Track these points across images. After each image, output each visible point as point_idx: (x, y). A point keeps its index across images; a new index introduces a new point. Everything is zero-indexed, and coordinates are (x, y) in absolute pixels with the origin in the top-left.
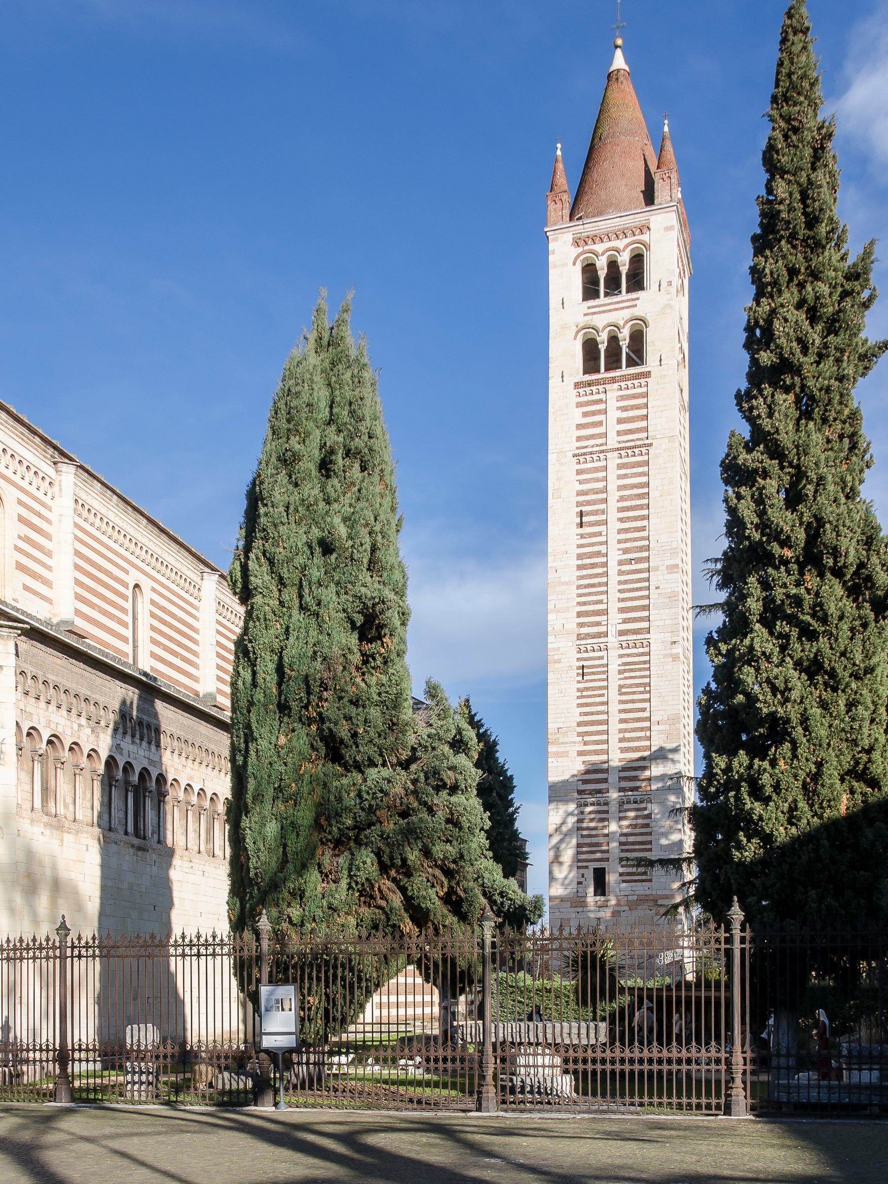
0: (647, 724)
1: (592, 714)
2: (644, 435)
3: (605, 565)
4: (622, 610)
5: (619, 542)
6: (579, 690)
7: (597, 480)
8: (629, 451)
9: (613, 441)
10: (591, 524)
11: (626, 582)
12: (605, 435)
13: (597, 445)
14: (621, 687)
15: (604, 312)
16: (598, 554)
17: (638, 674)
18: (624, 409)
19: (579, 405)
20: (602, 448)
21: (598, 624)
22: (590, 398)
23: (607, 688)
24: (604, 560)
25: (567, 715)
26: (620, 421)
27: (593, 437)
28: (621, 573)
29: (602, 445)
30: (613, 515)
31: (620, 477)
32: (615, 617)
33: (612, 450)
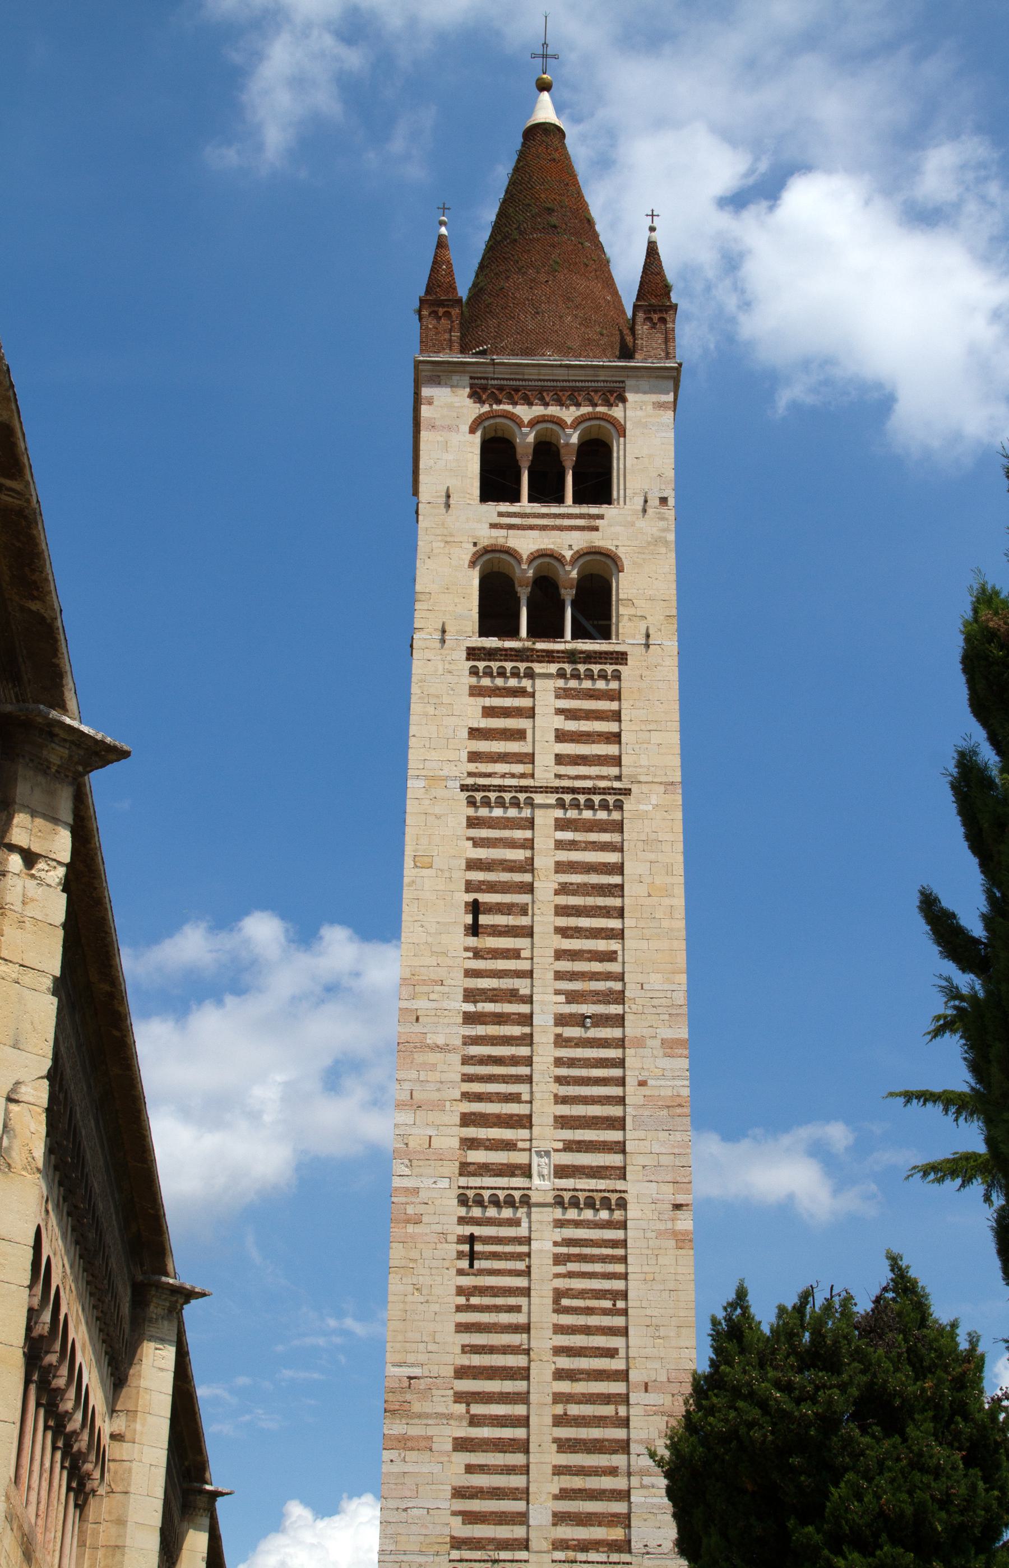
2: (614, 771)
3: (527, 1019)
4: (563, 1122)
5: (559, 976)
7: (512, 844)
8: (582, 798)
9: (545, 771)
10: (497, 931)
11: (572, 1063)
12: (529, 758)
13: (513, 776)
14: (559, 1294)
16: (513, 996)
17: (598, 1267)
18: (571, 714)
20: (524, 782)
21: (509, 1146)
23: (526, 1292)
24: (524, 1009)
25: (432, 1347)
26: (561, 736)
28: (561, 1041)
29: (523, 776)
31: (560, 845)
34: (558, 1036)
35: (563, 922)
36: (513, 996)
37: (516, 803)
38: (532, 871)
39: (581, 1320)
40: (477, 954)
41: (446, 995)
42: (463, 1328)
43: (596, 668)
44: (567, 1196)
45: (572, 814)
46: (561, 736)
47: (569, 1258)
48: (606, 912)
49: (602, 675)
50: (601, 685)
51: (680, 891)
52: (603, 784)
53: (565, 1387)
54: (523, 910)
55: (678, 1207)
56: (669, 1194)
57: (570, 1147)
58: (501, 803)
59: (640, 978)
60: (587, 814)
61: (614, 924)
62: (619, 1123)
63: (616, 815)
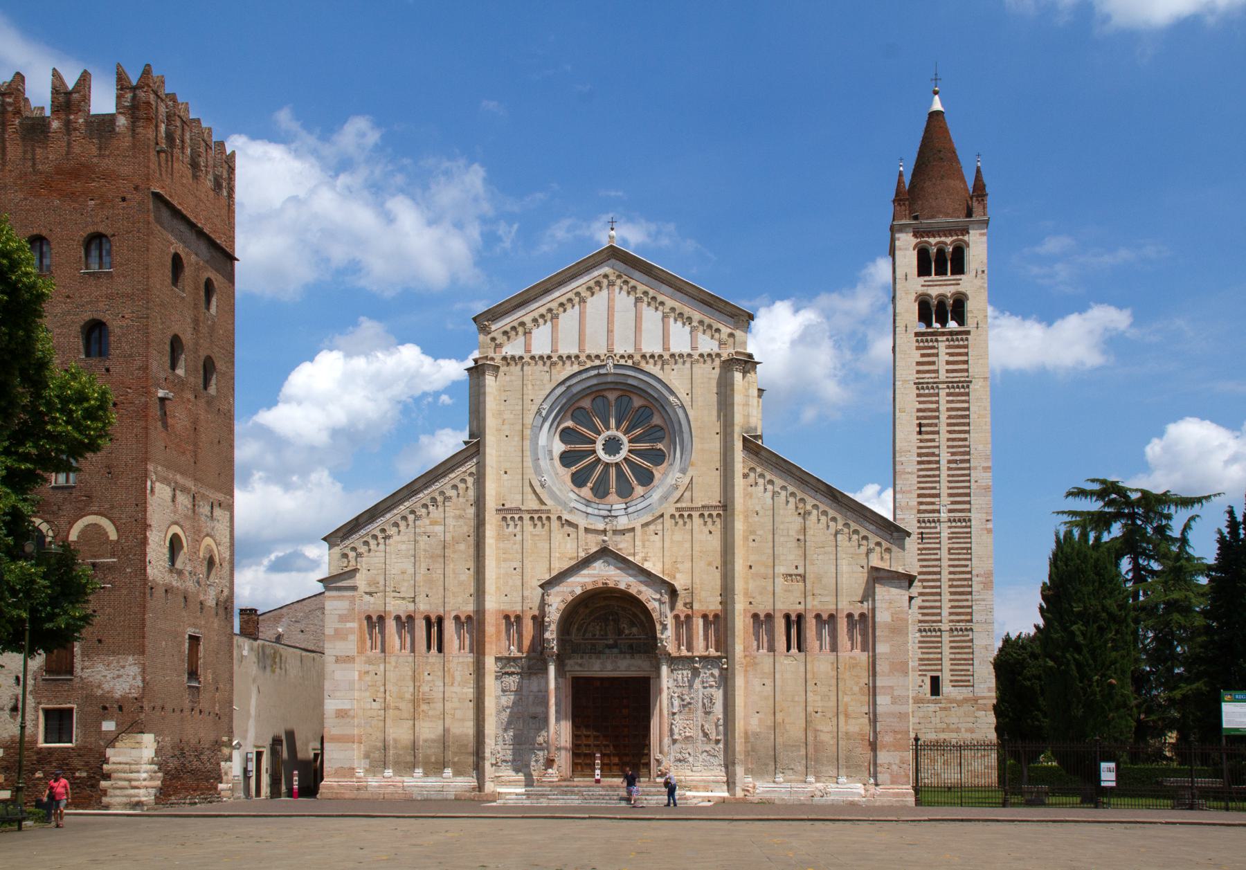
0: (969, 576)
1: (929, 566)
2: (966, 374)
3: (938, 462)
4: (950, 495)
6: (919, 549)
7: (932, 402)
8: (955, 385)
9: (943, 376)
10: (927, 433)
11: (953, 476)
12: (937, 371)
15: (936, 285)
16: (933, 454)
18: (951, 355)
19: (918, 348)
21: (933, 503)
22: (926, 344)
24: (937, 459)
26: (948, 363)
27: (928, 372)
28: (949, 469)
29: (935, 378)
30: (943, 428)
31: (948, 402)
32: (945, 499)
33: (943, 383)
34: (948, 467)
35: (950, 428)
36: (933, 454)
37: (933, 388)
38: (939, 411)
39: (957, 557)
40: (921, 441)
41: (912, 455)
42: (920, 560)
43: (959, 337)
44: (952, 519)
45: (952, 390)
46: (948, 363)
47: (953, 538)
48: (964, 424)
49: (962, 340)
50: (961, 343)
51: (989, 416)
52: (962, 379)
53: (952, 576)
54: (936, 425)
55: (988, 521)
56: (984, 517)
57: (953, 503)
58: (928, 388)
59: (976, 446)
60: (957, 390)
61: (966, 428)
62: (969, 495)
63: (967, 390)
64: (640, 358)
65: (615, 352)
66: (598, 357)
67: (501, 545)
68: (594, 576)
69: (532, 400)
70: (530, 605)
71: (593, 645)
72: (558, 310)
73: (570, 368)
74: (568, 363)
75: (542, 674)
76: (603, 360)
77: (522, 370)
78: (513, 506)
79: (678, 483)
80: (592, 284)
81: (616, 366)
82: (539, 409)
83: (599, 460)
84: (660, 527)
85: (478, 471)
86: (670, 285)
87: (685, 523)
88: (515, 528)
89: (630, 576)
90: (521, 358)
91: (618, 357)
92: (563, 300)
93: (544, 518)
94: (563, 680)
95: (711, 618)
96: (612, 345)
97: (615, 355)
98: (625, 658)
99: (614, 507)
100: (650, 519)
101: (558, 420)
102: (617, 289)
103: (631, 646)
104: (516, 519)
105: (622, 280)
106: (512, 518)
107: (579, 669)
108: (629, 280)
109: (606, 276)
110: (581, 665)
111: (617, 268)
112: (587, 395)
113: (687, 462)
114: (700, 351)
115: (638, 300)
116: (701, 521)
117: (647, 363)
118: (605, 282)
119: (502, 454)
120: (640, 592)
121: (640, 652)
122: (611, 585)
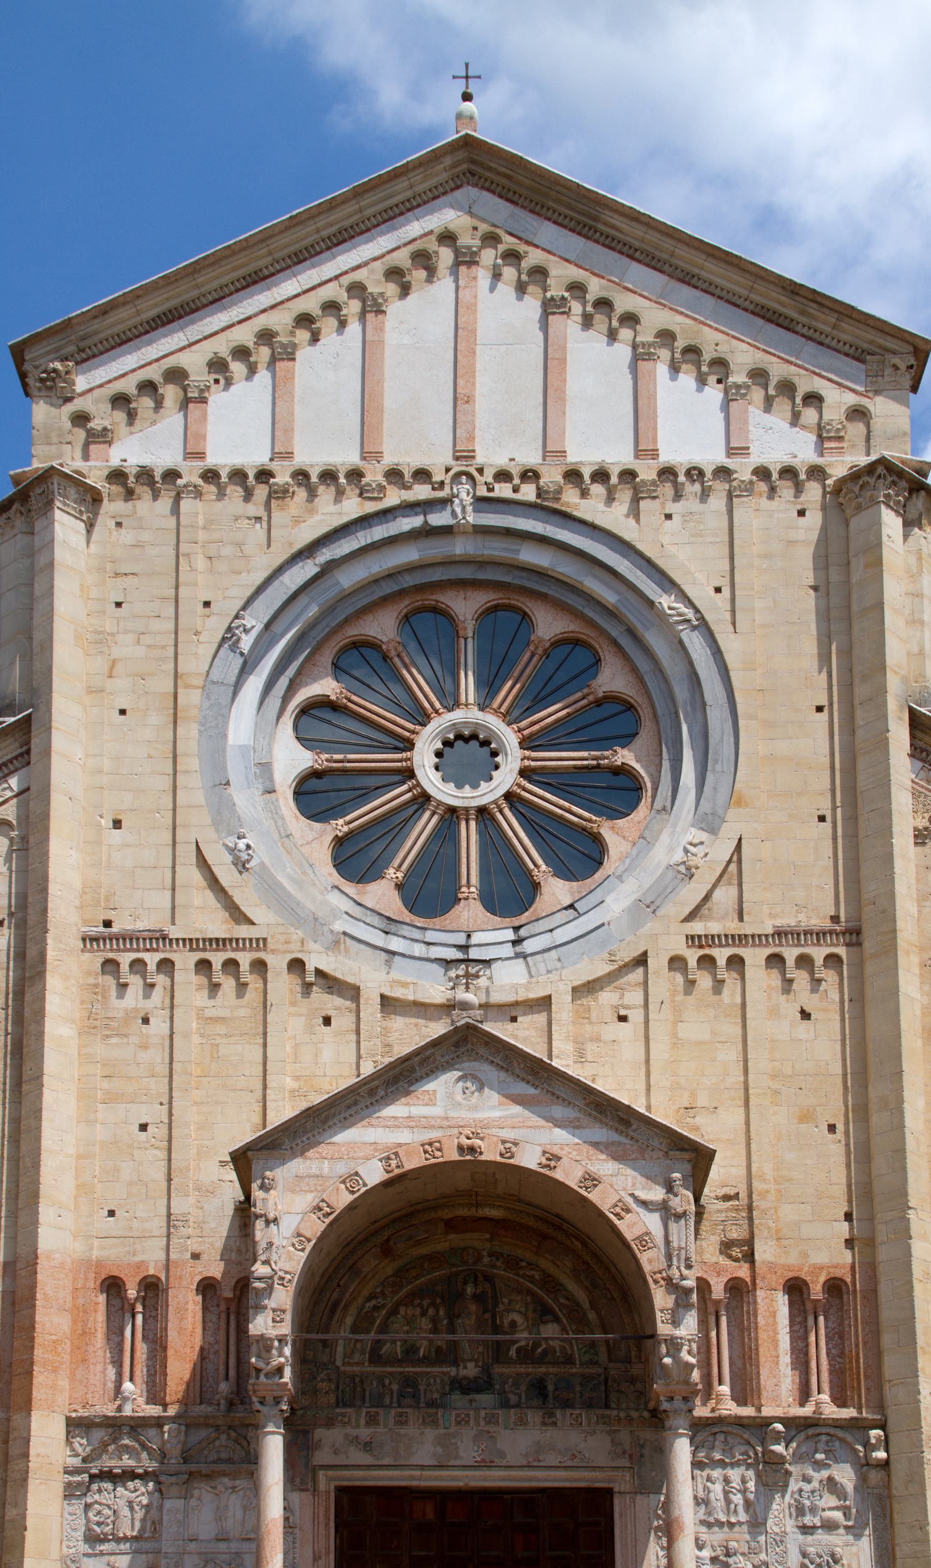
64: (560, 479)
65: (480, 459)
66: (422, 475)
67: (99, 1049)
68: (426, 1124)
69: (207, 604)
70: (194, 1245)
71: (409, 1382)
72: (292, 334)
73: (332, 508)
74: (326, 494)
75: (234, 1476)
76: (442, 483)
77: (176, 510)
78: (141, 925)
79: (693, 861)
80: (402, 258)
81: (482, 503)
82: (229, 629)
83: (423, 799)
84: (635, 997)
85: (24, 816)
86: (654, 262)
87: (719, 985)
88: (147, 996)
89: (558, 1124)
90: (172, 475)
91: (488, 477)
92: (311, 304)
93: (245, 966)
94: (307, 1497)
95: (817, 1291)
96: (471, 438)
97: (481, 471)
98: (522, 1422)
99: (476, 938)
100: (605, 969)
101: (291, 671)
102: (483, 277)
103: (539, 1389)
104: (152, 966)
105: (501, 248)
106: (138, 965)
107: (366, 1459)
108: (522, 248)
109: (447, 237)
110: (367, 1446)
111: (481, 212)
112: (385, 601)
113: (724, 792)
114: (756, 459)
115: (551, 307)
116: (774, 979)
117: (584, 494)
118: (446, 256)
119: (107, 765)
120: (591, 1180)
121: (567, 1404)
122: (490, 1154)
